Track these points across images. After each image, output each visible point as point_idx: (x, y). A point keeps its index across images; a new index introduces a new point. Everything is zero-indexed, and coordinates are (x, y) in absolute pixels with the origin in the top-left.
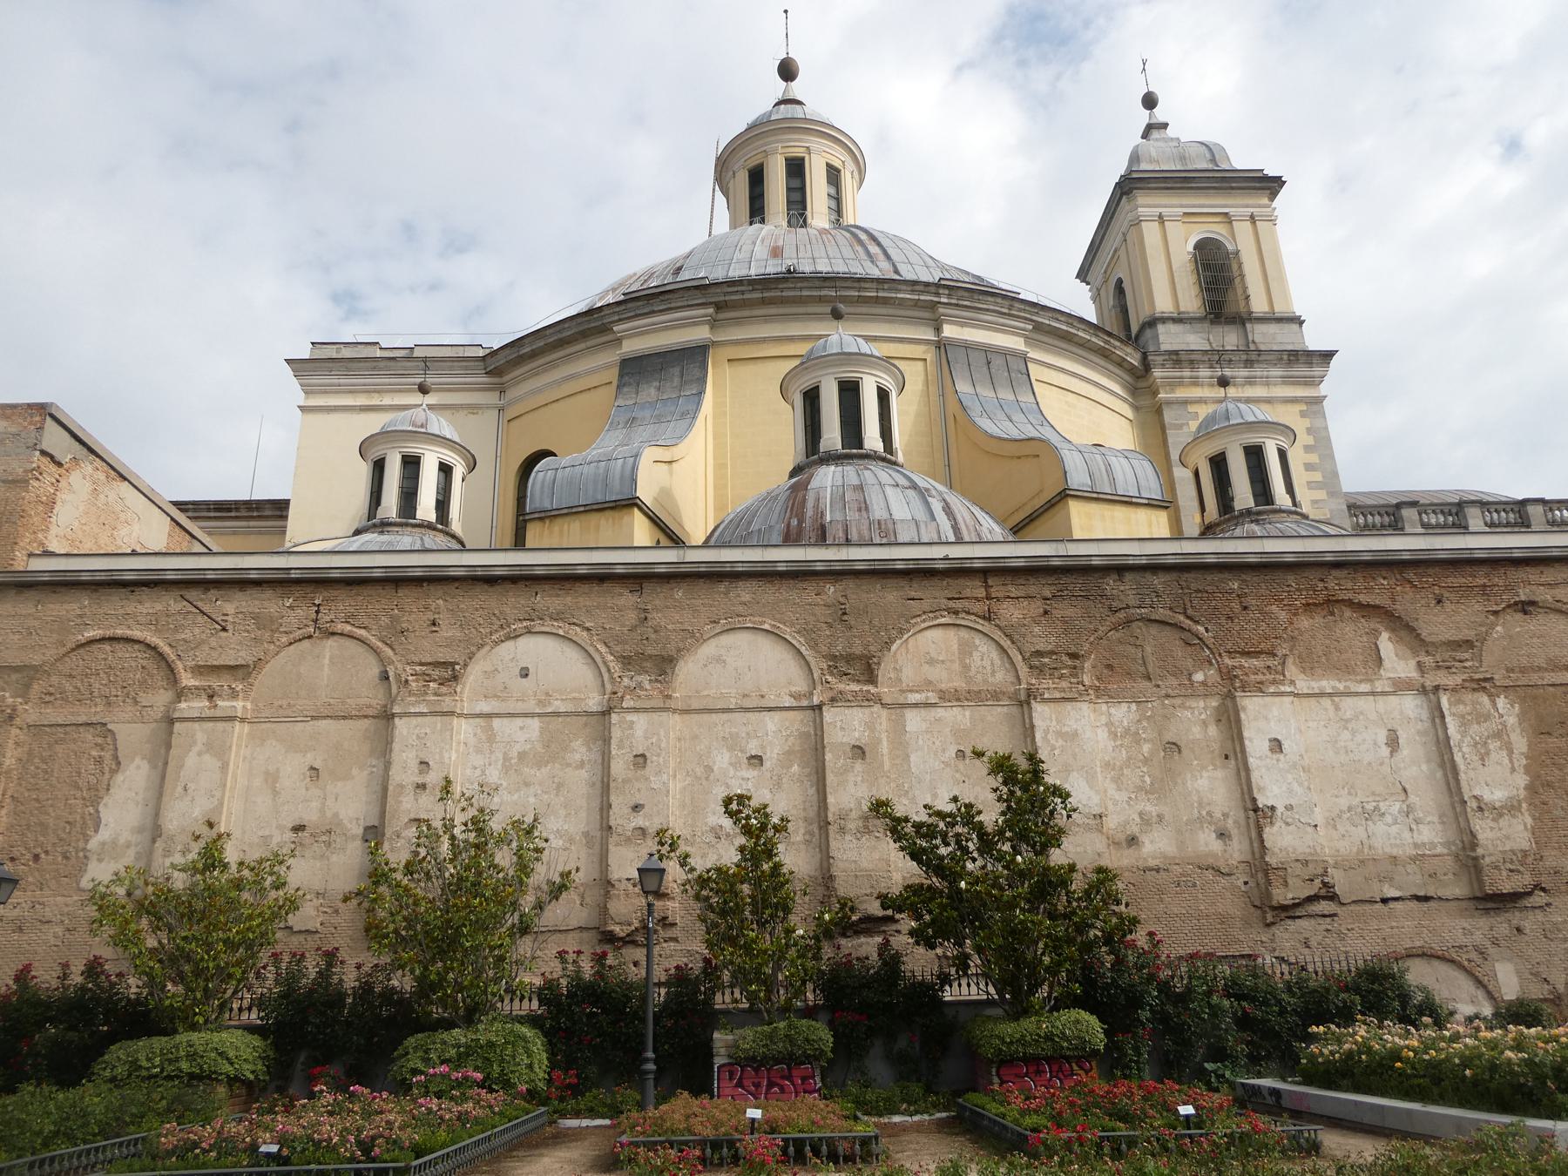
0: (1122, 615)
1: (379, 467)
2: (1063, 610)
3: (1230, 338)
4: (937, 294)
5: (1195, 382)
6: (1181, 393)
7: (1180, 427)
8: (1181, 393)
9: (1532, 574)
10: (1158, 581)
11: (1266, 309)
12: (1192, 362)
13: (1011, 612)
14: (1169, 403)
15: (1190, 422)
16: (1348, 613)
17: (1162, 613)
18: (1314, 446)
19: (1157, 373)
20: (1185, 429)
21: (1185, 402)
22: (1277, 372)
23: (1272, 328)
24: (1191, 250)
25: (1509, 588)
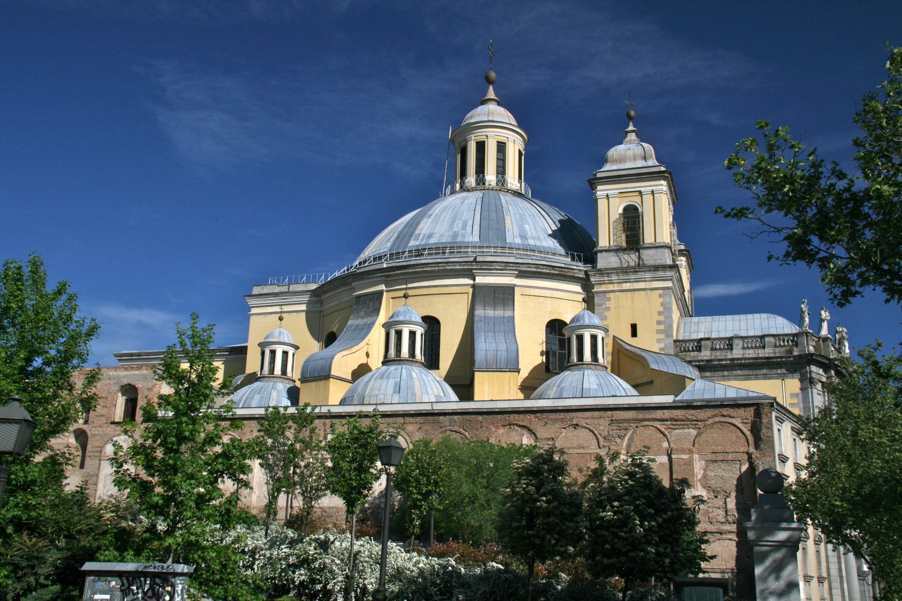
0: (443, 429)
1: (263, 354)
2: (426, 427)
3: (631, 259)
4: (471, 265)
5: (611, 283)
6: (603, 288)
7: (601, 305)
8: (603, 288)
9: (580, 414)
10: (456, 417)
11: (653, 241)
12: (608, 273)
13: (410, 428)
14: (597, 293)
15: (607, 303)
16: (516, 428)
17: (456, 428)
18: (663, 312)
19: (592, 279)
20: (604, 306)
21: (605, 292)
22: (648, 275)
23: (652, 252)
24: (621, 211)
25: (571, 419)
